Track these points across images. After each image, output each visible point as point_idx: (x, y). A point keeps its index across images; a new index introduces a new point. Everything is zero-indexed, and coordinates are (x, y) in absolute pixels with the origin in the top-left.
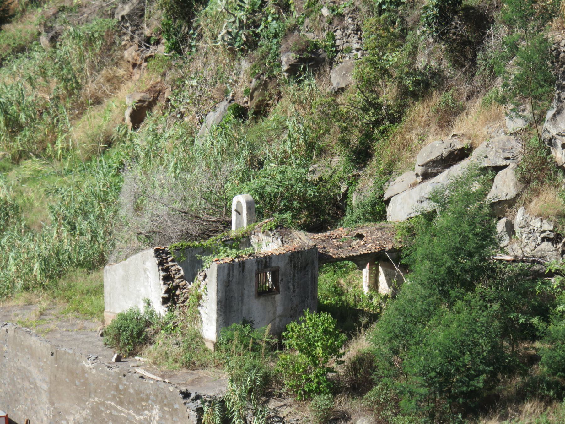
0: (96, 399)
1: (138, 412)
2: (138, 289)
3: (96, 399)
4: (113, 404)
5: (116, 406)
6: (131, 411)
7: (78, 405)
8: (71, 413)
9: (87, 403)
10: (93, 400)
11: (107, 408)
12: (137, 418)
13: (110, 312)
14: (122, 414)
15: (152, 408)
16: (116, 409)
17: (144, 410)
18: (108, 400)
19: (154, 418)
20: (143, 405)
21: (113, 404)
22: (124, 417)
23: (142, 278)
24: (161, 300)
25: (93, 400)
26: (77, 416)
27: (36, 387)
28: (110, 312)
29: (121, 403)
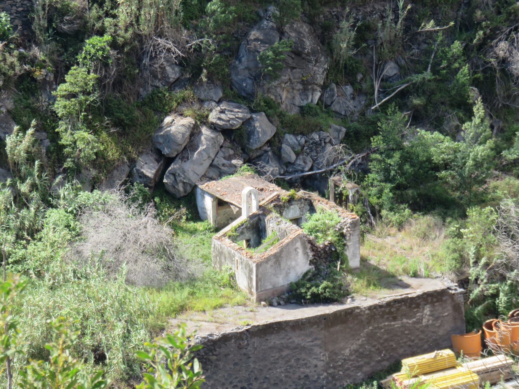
0: (371, 328)
1: (410, 318)
2: (289, 264)
3: (371, 328)
4: (386, 323)
5: (389, 323)
6: (405, 321)
7: (353, 339)
8: (347, 348)
9: (362, 334)
10: (367, 330)
11: (381, 328)
12: (410, 322)
13: (262, 291)
14: (396, 326)
15: (424, 309)
16: (391, 325)
17: (416, 314)
18: (381, 324)
19: (426, 314)
20: (414, 312)
21: (386, 323)
22: (398, 327)
23: (293, 256)
24: (309, 262)
25: (367, 330)
26: (354, 347)
27: (304, 348)
28: (262, 291)
29: (395, 319)
